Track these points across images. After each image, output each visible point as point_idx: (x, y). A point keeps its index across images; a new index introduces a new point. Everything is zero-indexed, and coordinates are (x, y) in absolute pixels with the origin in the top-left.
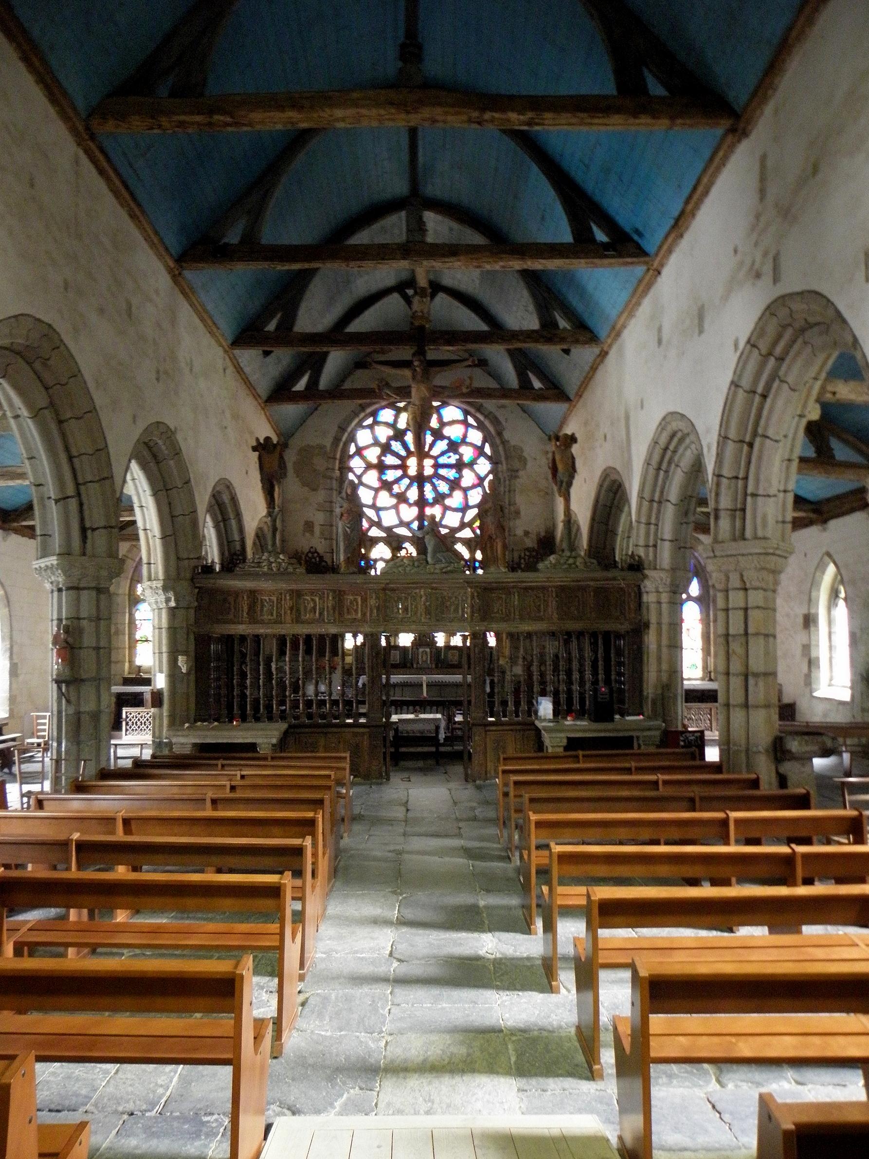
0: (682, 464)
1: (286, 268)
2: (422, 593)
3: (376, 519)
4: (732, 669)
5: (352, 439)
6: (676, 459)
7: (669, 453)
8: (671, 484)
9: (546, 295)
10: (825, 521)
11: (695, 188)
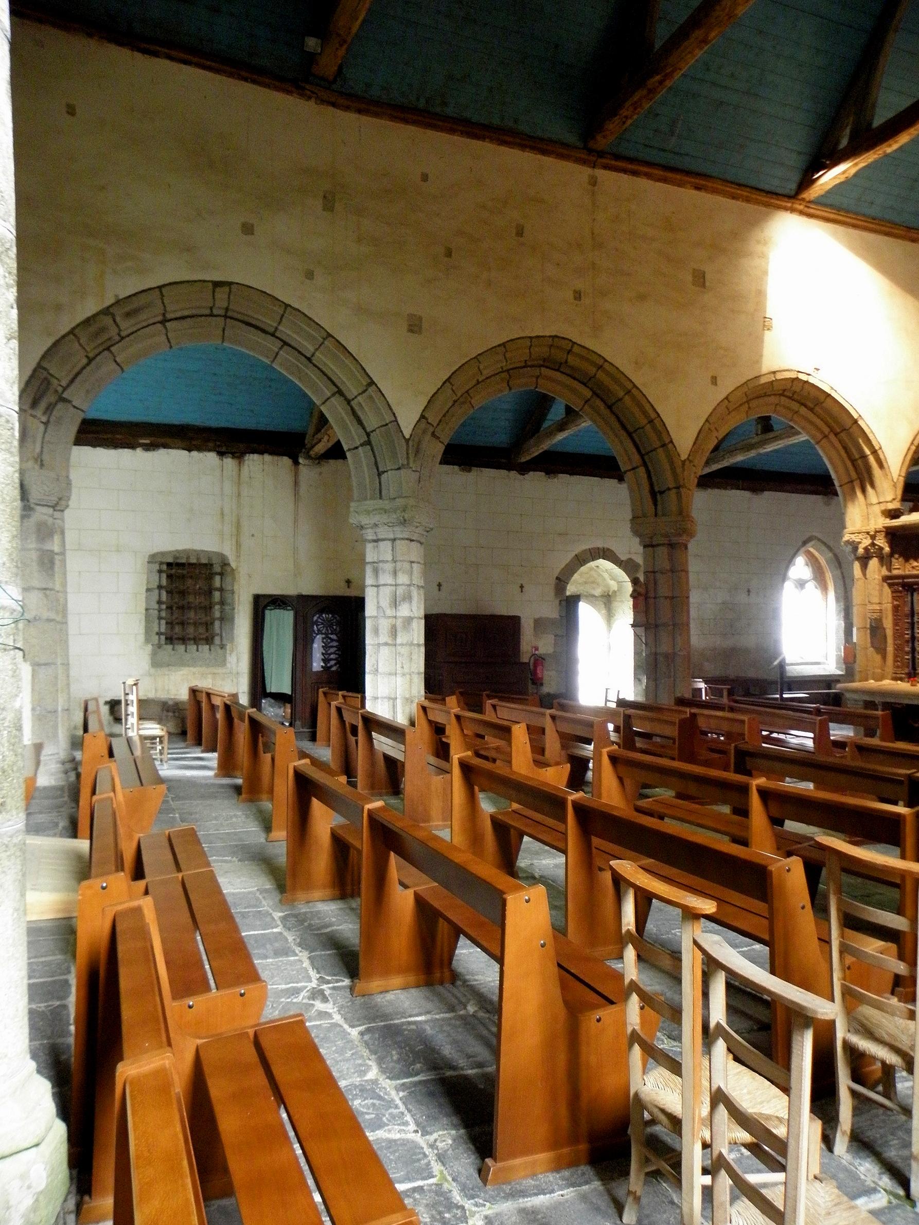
1: (895, 146)
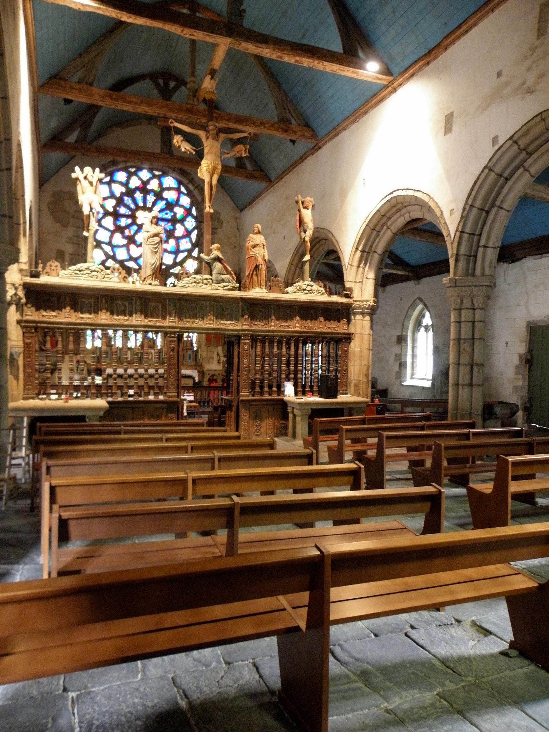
0: (392, 228)
2: (208, 304)
3: (111, 254)
4: (462, 361)
6: (389, 223)
7: (385, 219)
8: (380, 240)
9: (284, 98)
10: (419, 278)
11: (459, 27)
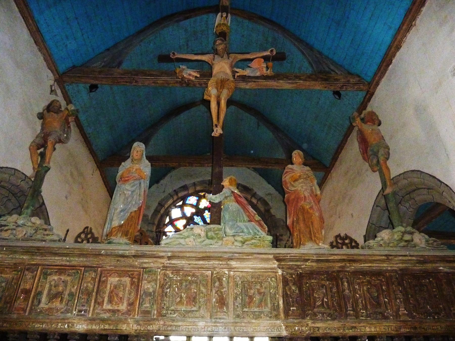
5: (168, 213)
